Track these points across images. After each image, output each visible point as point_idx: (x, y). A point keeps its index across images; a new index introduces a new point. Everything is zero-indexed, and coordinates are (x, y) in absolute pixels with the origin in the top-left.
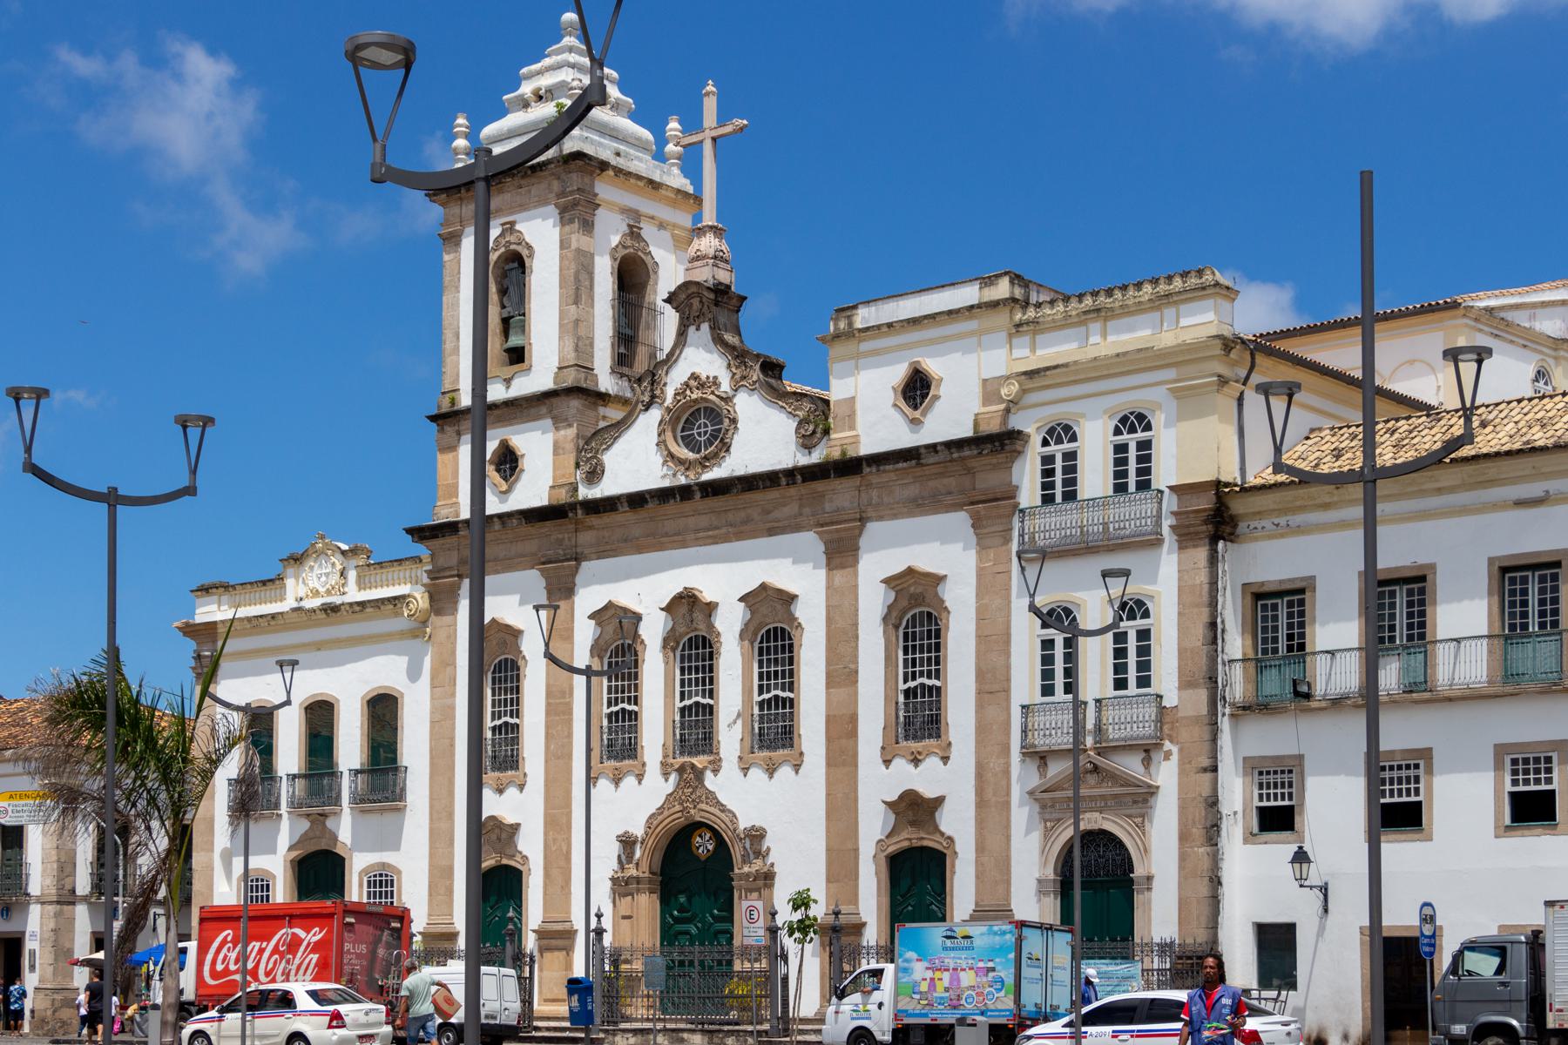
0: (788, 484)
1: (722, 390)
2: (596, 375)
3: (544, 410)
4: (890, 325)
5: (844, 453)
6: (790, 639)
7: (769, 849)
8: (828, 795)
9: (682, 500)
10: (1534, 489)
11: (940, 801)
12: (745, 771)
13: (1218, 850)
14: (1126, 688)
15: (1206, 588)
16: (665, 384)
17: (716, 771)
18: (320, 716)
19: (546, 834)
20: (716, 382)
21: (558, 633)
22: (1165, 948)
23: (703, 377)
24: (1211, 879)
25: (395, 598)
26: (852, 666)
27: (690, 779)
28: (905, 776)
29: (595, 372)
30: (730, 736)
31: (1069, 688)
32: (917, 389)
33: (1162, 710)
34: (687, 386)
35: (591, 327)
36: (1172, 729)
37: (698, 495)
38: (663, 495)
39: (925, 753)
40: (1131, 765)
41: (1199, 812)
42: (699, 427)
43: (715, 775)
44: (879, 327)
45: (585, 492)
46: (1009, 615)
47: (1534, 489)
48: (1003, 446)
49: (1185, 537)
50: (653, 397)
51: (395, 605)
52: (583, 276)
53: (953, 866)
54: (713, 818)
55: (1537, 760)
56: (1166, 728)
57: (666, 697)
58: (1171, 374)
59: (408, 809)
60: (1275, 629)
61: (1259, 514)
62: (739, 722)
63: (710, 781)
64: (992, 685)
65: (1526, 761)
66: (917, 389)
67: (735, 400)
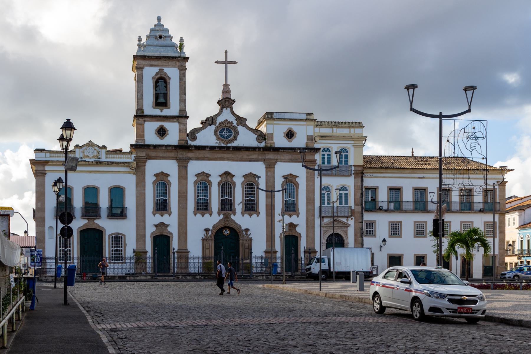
3: (175, 120)
4: (284, 119)
5: (271, 146)
9: (226, 150)
10: (421, 176)
11: (298, 225)
15: (360, 186)
17: (234, 215)
20: (232, 123)
23: (229, 121)
25: (125, 162)
27: (227, 218)
30: (239, 208)
32: (290, 135)
37: (231, 149)
38: (221, 148)
40: (344, 220)
41: (360, 230)
42: (225, 132)
44: (281, 119)
45: (190, 143)
46: (314, 187)
47: (421, 176)
48: (317, 151)
49: (356, 175)
51: (124, 164)
55: (421, 224)
58: (352, 142)
60: (368, 196)
63: (232, 217)
64: (310, 201)
65: (419, 224)
66: (290, 135)
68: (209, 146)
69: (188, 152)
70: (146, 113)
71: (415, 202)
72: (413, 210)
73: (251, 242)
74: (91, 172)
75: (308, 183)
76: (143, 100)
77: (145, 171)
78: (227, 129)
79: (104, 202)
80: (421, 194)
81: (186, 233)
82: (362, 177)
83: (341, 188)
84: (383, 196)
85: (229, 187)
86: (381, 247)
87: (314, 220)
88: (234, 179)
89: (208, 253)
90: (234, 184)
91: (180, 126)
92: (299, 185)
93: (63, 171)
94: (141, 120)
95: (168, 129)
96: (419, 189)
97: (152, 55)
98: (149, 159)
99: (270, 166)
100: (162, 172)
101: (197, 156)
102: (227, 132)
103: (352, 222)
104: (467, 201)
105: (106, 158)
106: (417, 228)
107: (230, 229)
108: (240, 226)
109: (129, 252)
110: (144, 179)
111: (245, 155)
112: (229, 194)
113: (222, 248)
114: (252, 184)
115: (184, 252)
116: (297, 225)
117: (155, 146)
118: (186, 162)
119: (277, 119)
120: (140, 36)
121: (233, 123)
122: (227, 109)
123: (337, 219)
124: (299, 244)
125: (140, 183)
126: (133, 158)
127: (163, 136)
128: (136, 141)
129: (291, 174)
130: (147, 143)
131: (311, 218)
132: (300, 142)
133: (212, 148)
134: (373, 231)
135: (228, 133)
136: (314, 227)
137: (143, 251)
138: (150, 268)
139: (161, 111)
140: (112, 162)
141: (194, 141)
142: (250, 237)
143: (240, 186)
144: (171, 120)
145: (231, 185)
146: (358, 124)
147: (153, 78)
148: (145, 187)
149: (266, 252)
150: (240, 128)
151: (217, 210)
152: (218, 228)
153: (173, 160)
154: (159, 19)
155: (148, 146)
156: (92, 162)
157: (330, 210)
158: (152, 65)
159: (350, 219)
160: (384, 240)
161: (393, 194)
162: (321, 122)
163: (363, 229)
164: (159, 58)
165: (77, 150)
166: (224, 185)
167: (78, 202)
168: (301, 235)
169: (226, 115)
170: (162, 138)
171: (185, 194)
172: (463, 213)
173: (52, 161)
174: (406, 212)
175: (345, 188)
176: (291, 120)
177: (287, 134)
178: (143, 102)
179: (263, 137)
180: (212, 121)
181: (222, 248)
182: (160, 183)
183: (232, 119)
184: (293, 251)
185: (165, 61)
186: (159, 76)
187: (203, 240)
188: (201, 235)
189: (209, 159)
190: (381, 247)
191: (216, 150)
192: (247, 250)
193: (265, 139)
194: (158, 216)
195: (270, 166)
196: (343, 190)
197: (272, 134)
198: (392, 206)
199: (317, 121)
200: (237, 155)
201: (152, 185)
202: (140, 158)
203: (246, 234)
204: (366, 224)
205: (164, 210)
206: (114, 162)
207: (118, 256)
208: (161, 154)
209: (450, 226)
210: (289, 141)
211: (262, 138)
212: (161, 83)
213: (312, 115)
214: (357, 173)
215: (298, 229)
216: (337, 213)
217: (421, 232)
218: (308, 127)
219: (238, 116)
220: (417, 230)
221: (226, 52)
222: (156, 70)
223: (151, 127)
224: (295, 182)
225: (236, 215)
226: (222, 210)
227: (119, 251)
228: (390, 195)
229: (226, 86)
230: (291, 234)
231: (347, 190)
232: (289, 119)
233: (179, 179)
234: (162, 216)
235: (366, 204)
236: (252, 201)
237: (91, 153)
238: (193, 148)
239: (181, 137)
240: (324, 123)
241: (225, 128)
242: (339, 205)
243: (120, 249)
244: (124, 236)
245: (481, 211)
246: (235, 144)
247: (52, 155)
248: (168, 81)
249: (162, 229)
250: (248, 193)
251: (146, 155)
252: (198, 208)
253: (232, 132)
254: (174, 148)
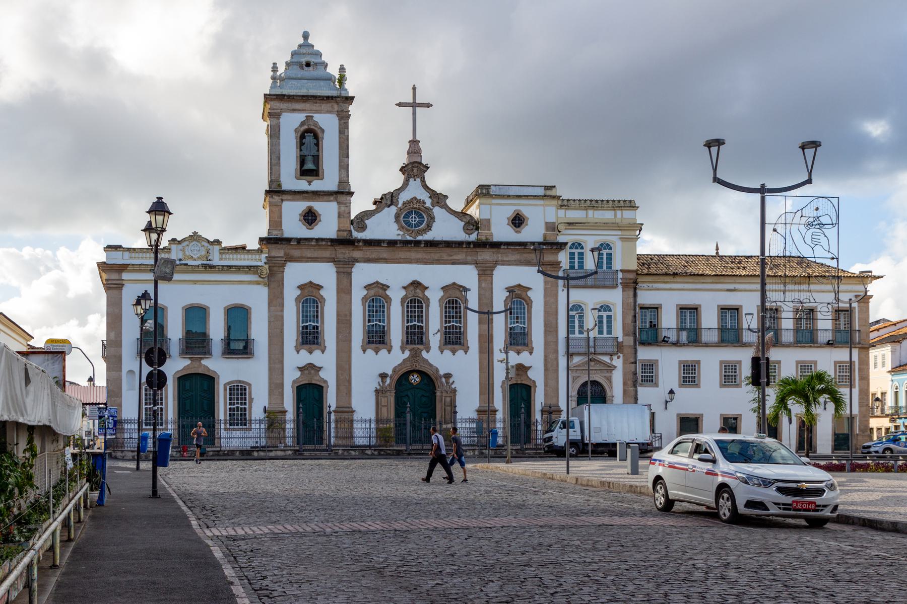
0: (466, 247)
3: (332, 198)
4: (509, 196)
5: (487, 239)
8: (480, 363)
9: (414, 246)
10: (731, 286)
14: (603, 334)
15: (633, 304)
17: (428, 352)
19: (337, 372)
20: (424, 203)
21: (344, 290)
25: (251, 266)
27: (415, 355)
30: (435, 339)
32: (518, 221)
37: (423, 245)
38: (406, 243)
40: (606, 359)
41: (631, 376)
42: (412, 218)
44: (504, 195)
45: (356, 235)
47: (731, 286)
48: (561, 247)
49: (625, 286)
55: (732, 366)
58: (619, 233)
60: (645, 319)
61: (643, 282)
62: (439, 333)
63: (424, 354)
64: (550, 328)
65: (729, 366)
66: (518, 221)
68: (386, 240)
69: (353, 250)
70: (285, 187)
71: (722, 330)
72: (719, 343)
73: (455, 395)
74: (195, 282)
75: (548, 299)
76: (280, 166)
77: (283, 280)
78: (415, 211)
79: (217, 330)
80: (731, 316)
81: (350, 381)
82: (635, 289)
83: (602, 307)
84: (669, 320)
85: (418, 306)
86: (667, 402)
87: (557, 359)
88: (427, 293)
89: (384, 414)
90: (427, 300)
91: (339, 208)
92: (532, 302)
93: (151, 280)
94: (277, 198)
95: (320, 213)
96: (729, 309)
97: (294, 94)
98: (290, 261)
99: (485, 273)
100: (311, 282)
101: (366, 257)
102: (415, 218)
103: (618, 362)
104: (807, 327)
105: (221, 259)
106: (725, 372)
107: (421, 373)
109: (257, 411)
110: (282, 293)
111: (445, 253)
112: (418, 317)
113: (409, 405)
114: (456, 301)
115: (346, 412)
117: (299, 241)
118: (350, 266)
119: (496, 195)
120: (274, 64)
121: (425, 203)
122: (415, 180)
123: (595, 357)
124: (532, 398)
125: (276, 300)
126: (264, 260)
127: (312, 223)
128: (269, 233)
129: (519, 285)
130: (287, 235)
131: (552, 356)
132: (533, 232)
133: (392, 243)
134: (654, 377)
135: (417, 219)
136: (557, 371)
137: (280, 409)
138: (290, 437)
139: (310, 184)
140: (230, 267)
141: (361, 232)
142: (453, 386)
143: (438, 304)
144: (325, 197)
145: (421, 303)
146: (628, 204)
147: (296, 131)
148: (283, 306)
149: (479, 411)
150: (437, 211)
151: (400, 344)
152: (401, 373)
153: (328, 262)
154: (306, 36)
155: (288, 240)
156: (198, 266)
157: (584, 343)
158: (294, 110)
159: (615, 357)
160: (671, 392)
161: (685, 316)
162: (568, 200)
163: (636, 374)
164: (305, 98)
165: (174, 247)
166: (411, 303)
167: (175, 331)
169: (414, 191)
170: (310, 227)
171: (348, 318)
172: (800, 347)
173: (133, 265)
174: (707, 345)
175: (608, 306)
176: (519, 197)
177: (512, 220)
178: (279, 170)
179: (473, 226)
180: (392, 200)
181: (409, 405)
182: (307, 299)
183: (424, 196)
184: (523, 410)
185: (316, 103)
186: (306, 127)
187: (377, 391)
188: (375, 383)
189: (386, 261)
190: (667, 402)
192: (448, 409)
193: (477, 229)
194: (303, 352)
195: (485, 273)
196: (605, 311)
197: (488, 221)
198: (684, 336)
199: (561, 198)
200: (432, 255)
201: (294, 303)
202: (276, 259)
203: (447, 383)
204: (642, 365)
205: (314, 344)
206: (232, 266)
207: (239, 419)
208: (309, 253)
209: (780, 368)
210: (516, 232)
211: (472, 226)
212: (309, 139)
213: (554, 190)
214: (625, 283)
216: (594, 348)
217: (732, 379)
218: (547, 208)
219: (433, 191)
220: (725, 376)
221: (414, 89)
222: (301, 117)
223: (293, 210)
224: (526, 298)
226: (408, 343)
227: (241, 411)
228: (681, 319)
229: (414, 142)
230: (519, 382)
231: (610, 310)
232: (517, 196)
233: (338, 292)
234: (311, 353)
235: (642, 332)
236: (456, 329)
237: (195, 252)
238: (361, 244)
239: (341, 225)
240: (572, 201)
241: (412, 211)
242: (597, 335)
243: (243, 406)
244: (250, 385)
245: (829, 344)
246: (428, 236)
247: (133, 255)
248: (320, 135)
249: (310, 373)
250: (449, 316)
251: (285, 254)
252: (369, 341)
253: (423, 218)
254: (329, 244)
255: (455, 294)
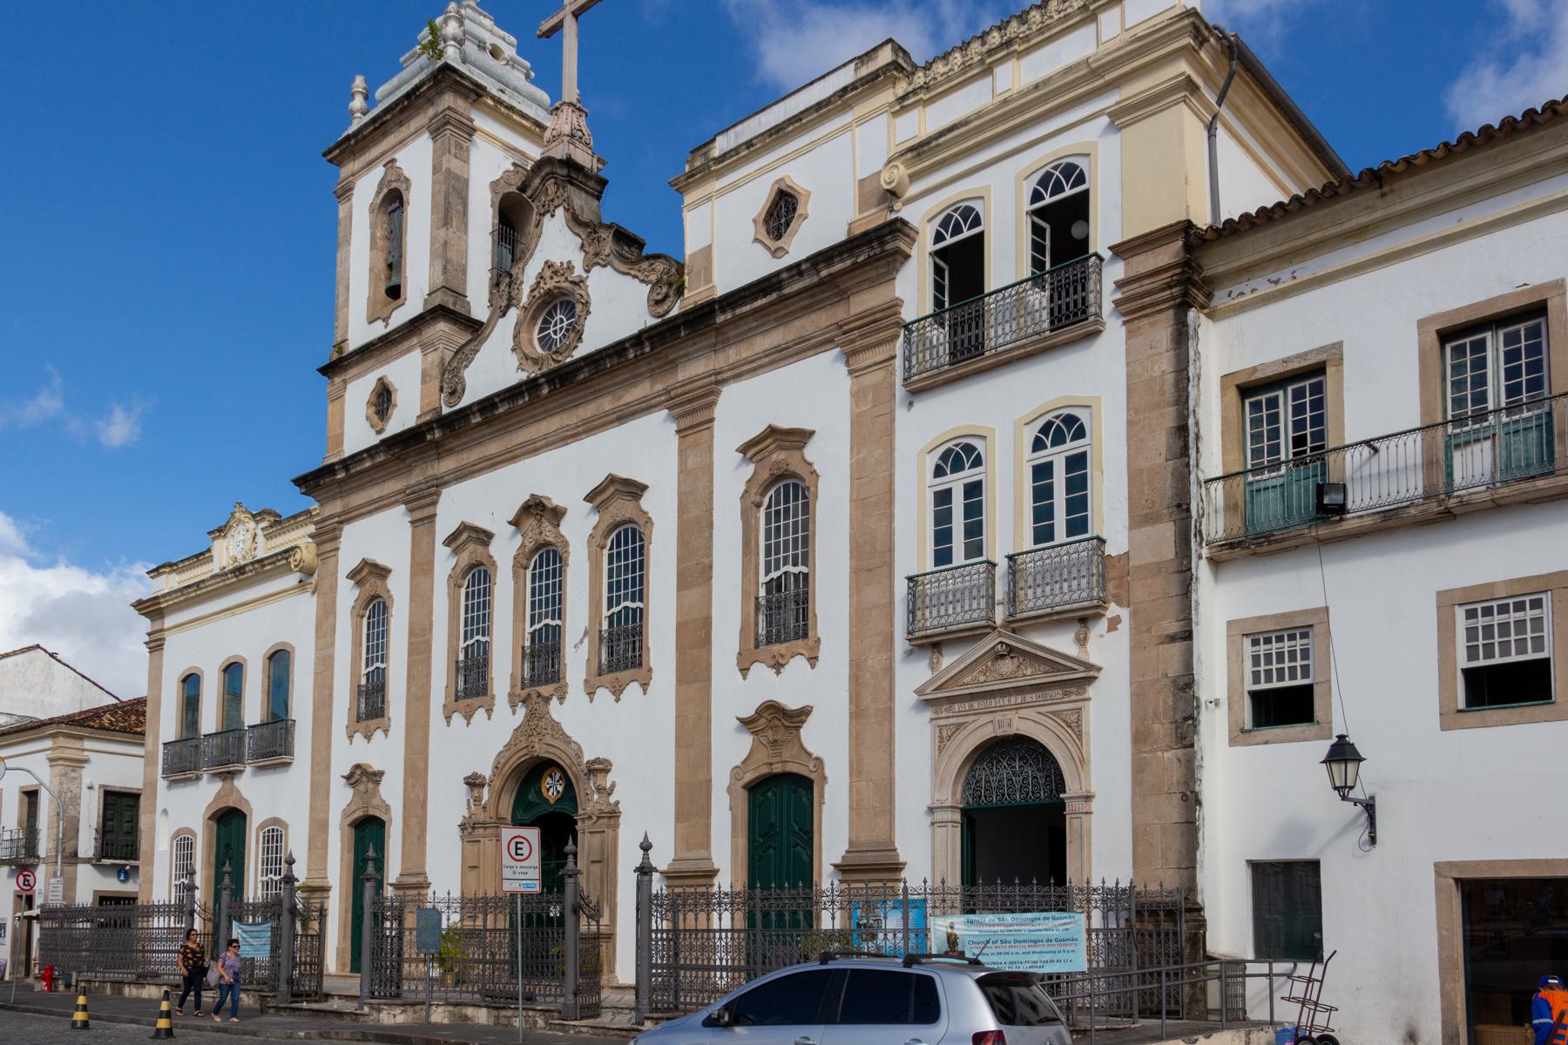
1: (576, 274)
2: (469, 303)
6: (641, 540)
7: (613, 785)
8: (678, 717)
12: (591, 694)
13: (1195, 752)
16: (522, 282)
17: (562, 699)
18: (233, 671)
20: (570, 268)
21: (422, 567)
22: (1114, 899)
24: (1184, 797)
26: (706, 561)
28: (765, 685)
29: (468, 299)
30: (576, 659)
31: (974, 549)
33: (1106, 560)
34: (541, 277)
35: (464, 253)
36: (1119, 586)
39: (790, 654)
40: (1062, 642)
41: (1164, 699)
43: (561, 703)
50: (510, 299)
52: (454, 199)
53: (822, 795)
54: (558, 752)
56: (1111, 587)
57: (515, 620)
59: (295, 762)
62: (586, 641)
63: (555, 710)
67: (588, 282)
78: (562, 303)
87: (889, 670)
95: (396, 387)
98: (348, 521)
108: (579, 753)
116: (804, 712)
118: (428, 500)
131: (874, 661)
168: (827, 772)
187: (463, 827)
191: (501, 410)
196: (1059, 440)
215: (813, 737)
225: (568, 696)
230: (778, 769)
255: (621, 508)
